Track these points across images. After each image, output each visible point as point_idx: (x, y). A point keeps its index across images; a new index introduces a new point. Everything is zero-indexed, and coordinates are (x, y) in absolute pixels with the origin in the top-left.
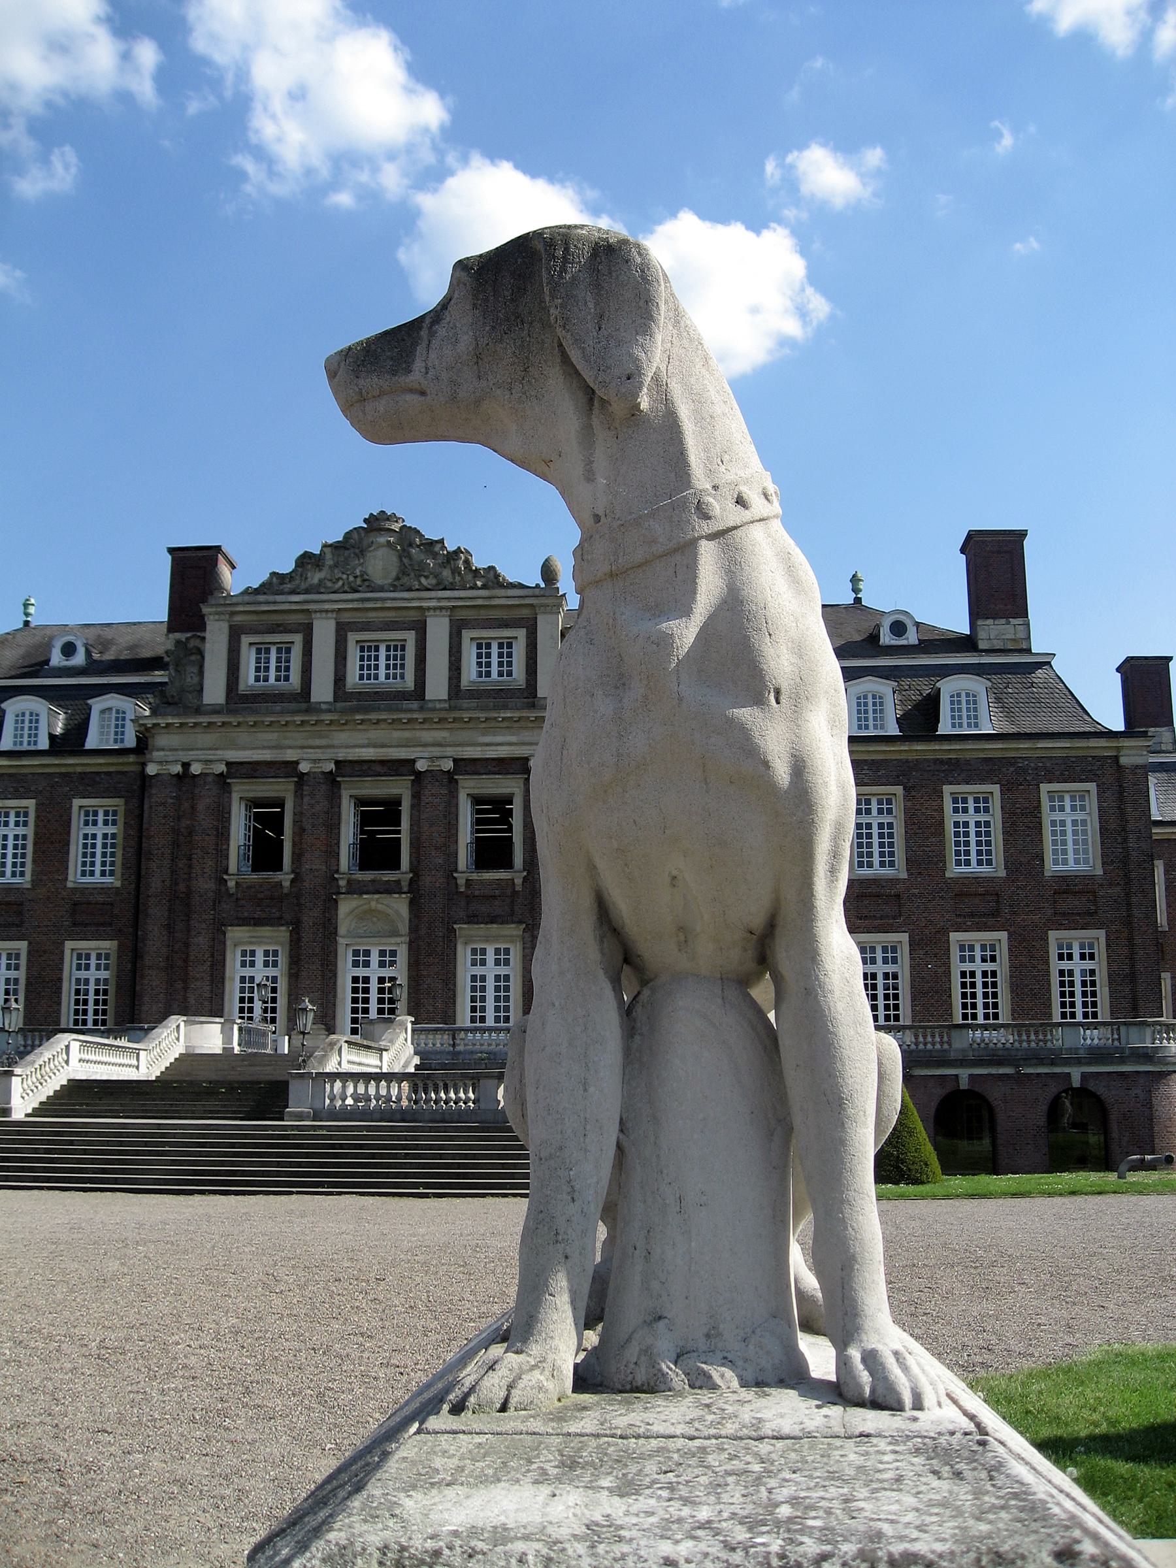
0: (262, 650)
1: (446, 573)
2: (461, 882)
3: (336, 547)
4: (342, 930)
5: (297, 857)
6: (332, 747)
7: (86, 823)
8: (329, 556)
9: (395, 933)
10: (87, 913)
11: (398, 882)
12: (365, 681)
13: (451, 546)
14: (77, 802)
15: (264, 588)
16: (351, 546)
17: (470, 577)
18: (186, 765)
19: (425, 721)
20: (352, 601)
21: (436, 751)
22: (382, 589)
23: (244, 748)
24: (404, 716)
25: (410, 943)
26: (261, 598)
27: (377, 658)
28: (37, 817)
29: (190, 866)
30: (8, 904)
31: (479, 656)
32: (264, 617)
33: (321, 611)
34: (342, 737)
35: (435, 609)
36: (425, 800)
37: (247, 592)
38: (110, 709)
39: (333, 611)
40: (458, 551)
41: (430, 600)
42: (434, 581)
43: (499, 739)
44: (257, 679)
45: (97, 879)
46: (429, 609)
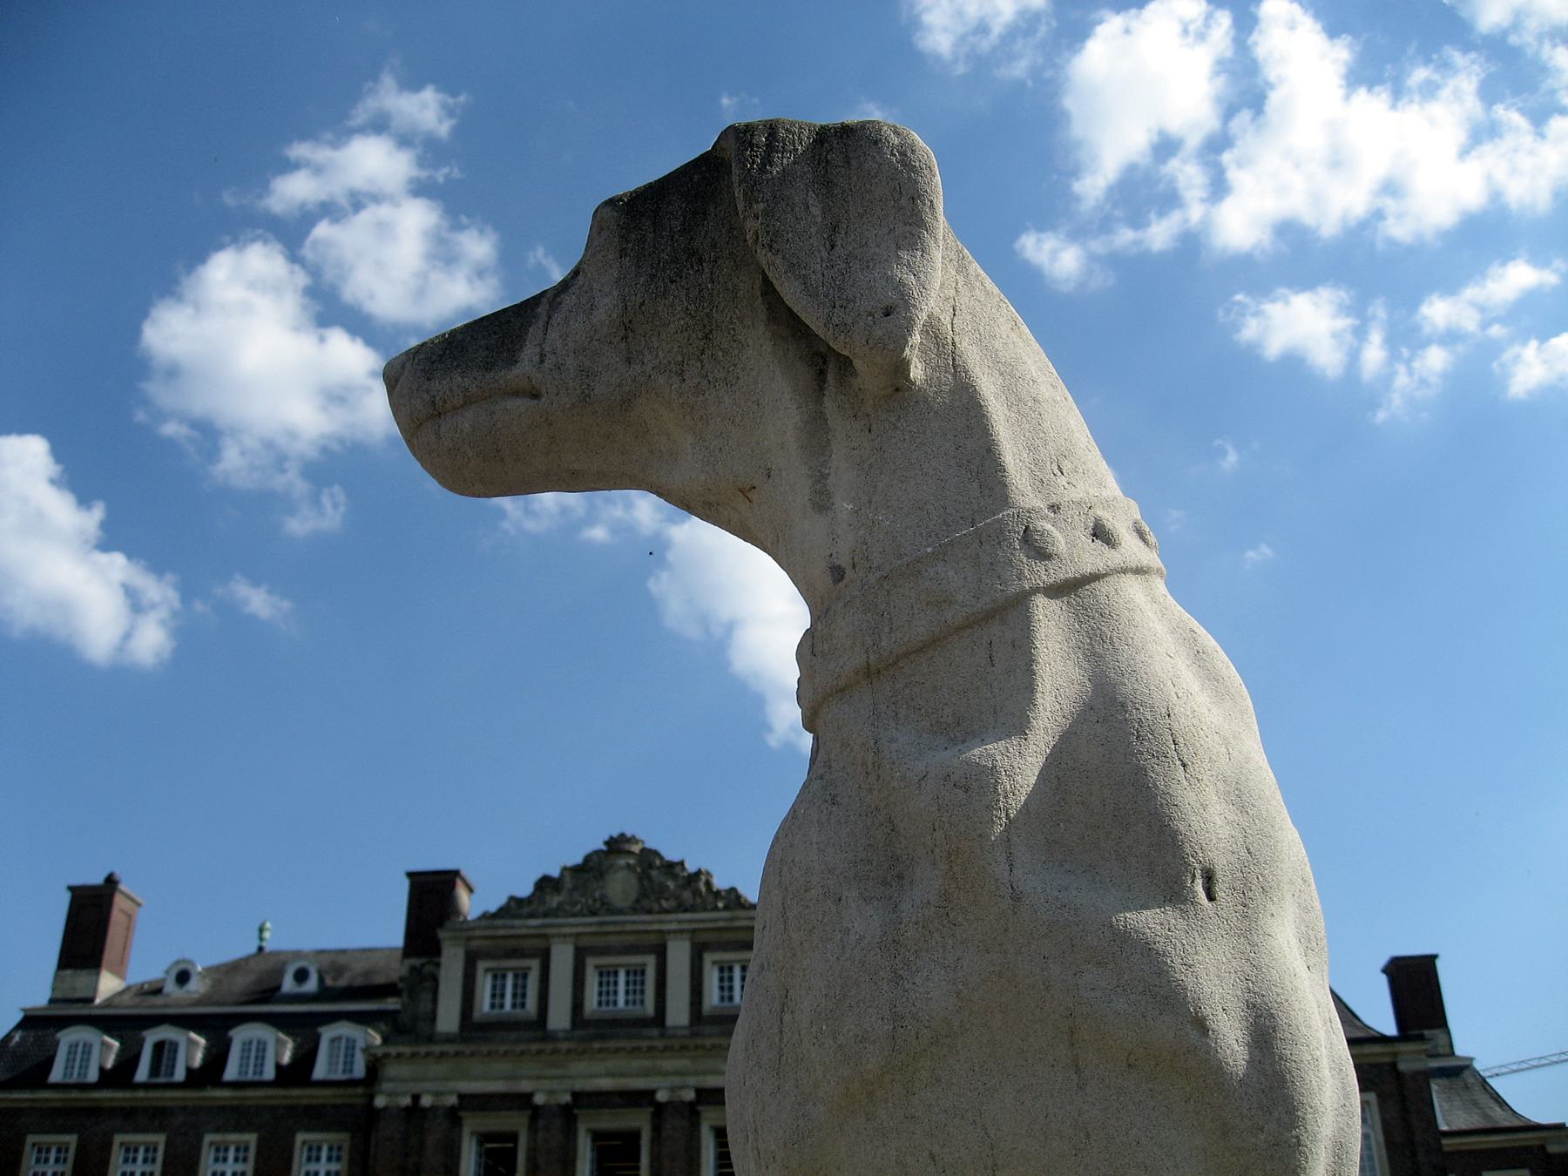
0: (499, 976)
1: (687, 895)
3: (577, 870)
6: (569, 1077)
7: (309, 1159)
8: (568, 879)
12: (604, 1008)
13: (691, 867)
14: (300, 1137)
15: (503, 912)
16: (591, 869)
17: (710, 899)
18: (416, 1098)
19: (666, 1049)
21: (676, 1080)
22: (621, 912)
23: (477, 1078)
24: (644, 1044)
26: (499, 922)
27: (616, 983)
28: (258, 1153)
31: (721, 979)
33: (559, 936)
34: (579, 1067)
35: (675, 932)
37: (485, 916)
38: (339, 1038)
39: (571, 935)
40: (699, 873)
41: (672, 922)
42: (673, 903)
44: (493, 1006)
46: (669, 932)
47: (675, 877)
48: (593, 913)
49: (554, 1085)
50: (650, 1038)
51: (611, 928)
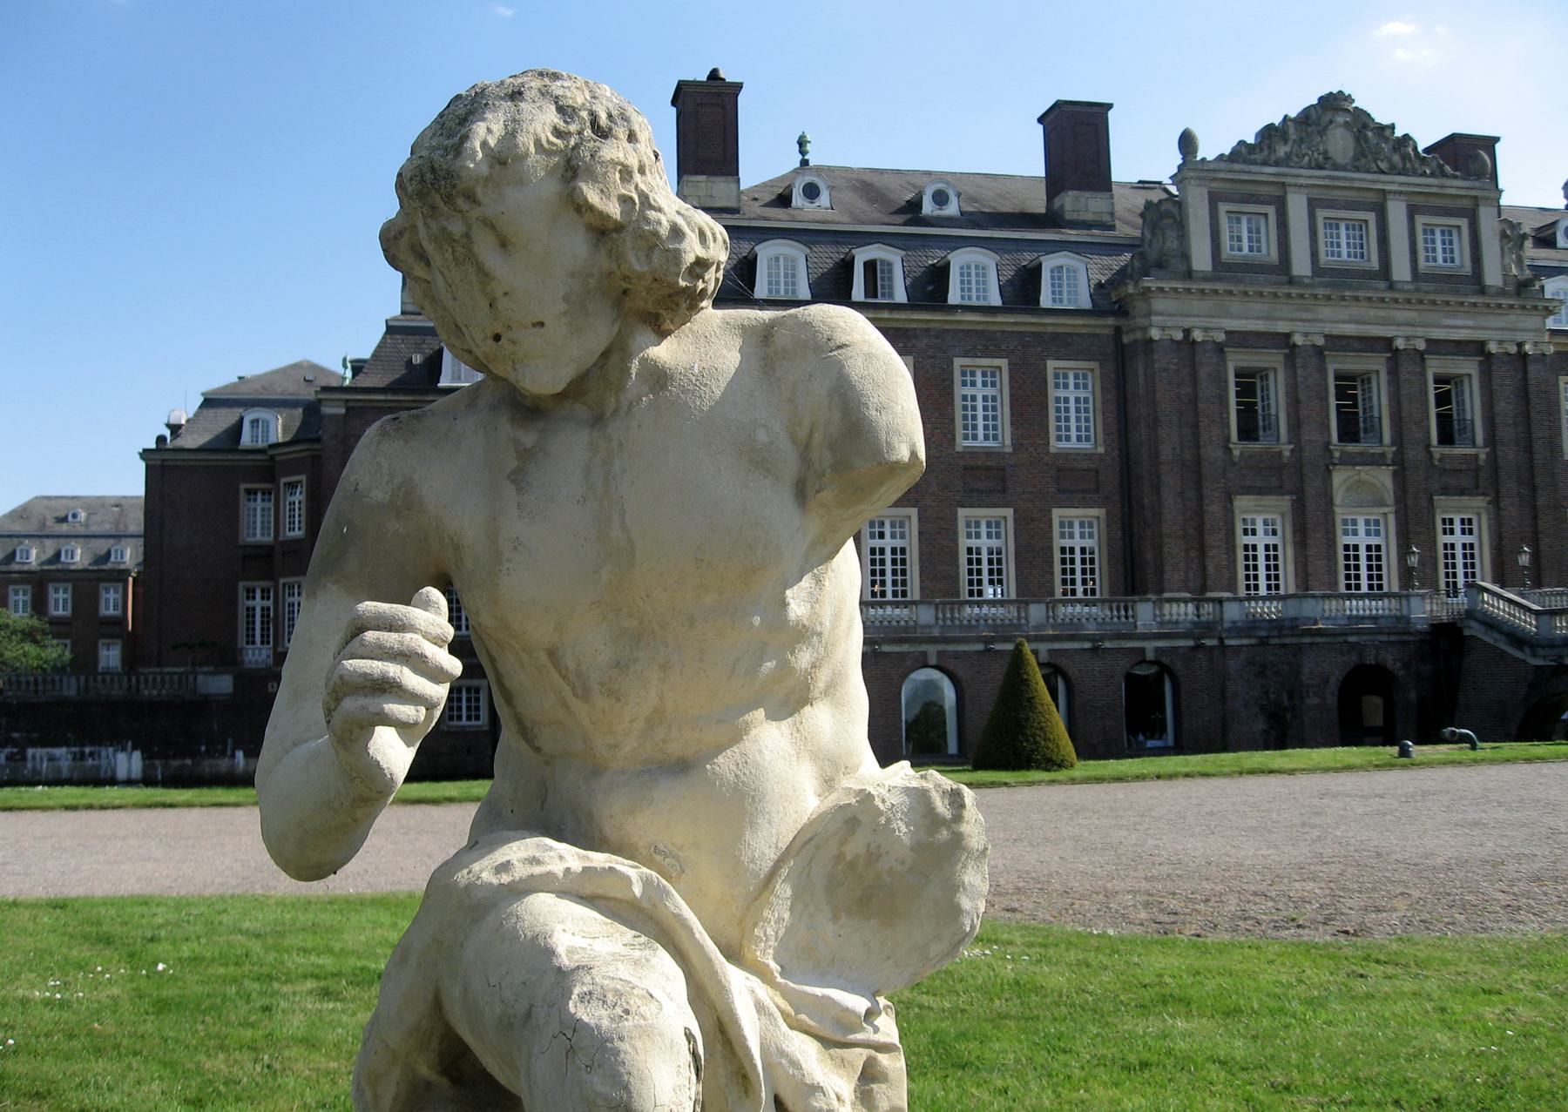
2: (1437, 456)
3: (1293, 120)
4: (1338, 500)
5: (1295, 426)
9: (1382, 504)
10: (1072, 480)
11: (1383, 455)
13: (1399, 133)
14: (1051, 365)
18: (1187, 332)
20: (1324, 178)
21: (1408, 331)
22: (1344, 168)
23: (1239, 318)
25: (1397, 512)
26: (1237, 167)
29: (1196, 435)
30: (989, 469)
32: (1238, 186)
34: (1325, 312)
35: (1395, 192)
36: (1403, 377)
39: (1306, 186)
40: (1406, 137)
41: (1393, 182)
43: (1459, 322)
45: (1073, 444)
46: (1390, 192)
47: (1386, 139)
48: (1320, 167)
49: (1307, 327)
50: (1377, 290)
51: (1337, 183)
